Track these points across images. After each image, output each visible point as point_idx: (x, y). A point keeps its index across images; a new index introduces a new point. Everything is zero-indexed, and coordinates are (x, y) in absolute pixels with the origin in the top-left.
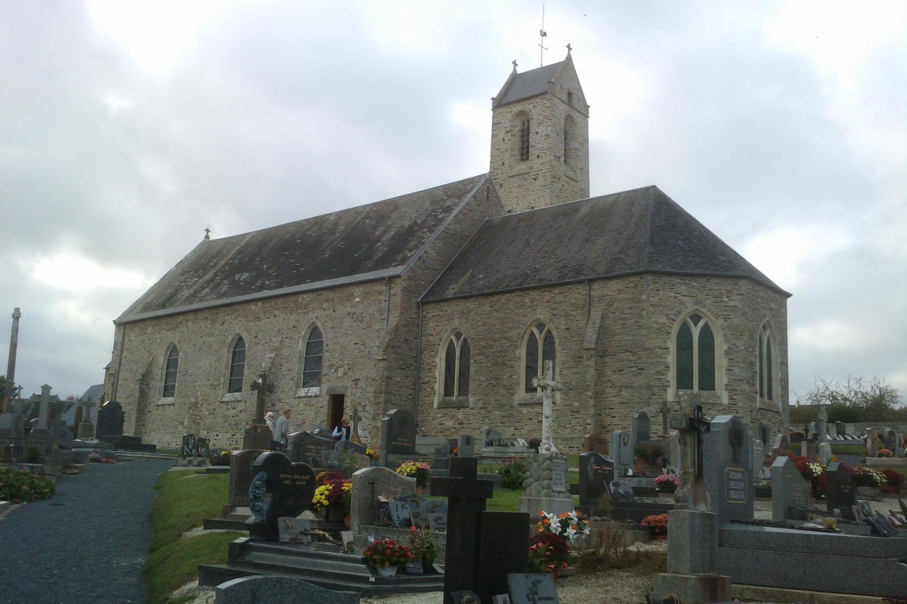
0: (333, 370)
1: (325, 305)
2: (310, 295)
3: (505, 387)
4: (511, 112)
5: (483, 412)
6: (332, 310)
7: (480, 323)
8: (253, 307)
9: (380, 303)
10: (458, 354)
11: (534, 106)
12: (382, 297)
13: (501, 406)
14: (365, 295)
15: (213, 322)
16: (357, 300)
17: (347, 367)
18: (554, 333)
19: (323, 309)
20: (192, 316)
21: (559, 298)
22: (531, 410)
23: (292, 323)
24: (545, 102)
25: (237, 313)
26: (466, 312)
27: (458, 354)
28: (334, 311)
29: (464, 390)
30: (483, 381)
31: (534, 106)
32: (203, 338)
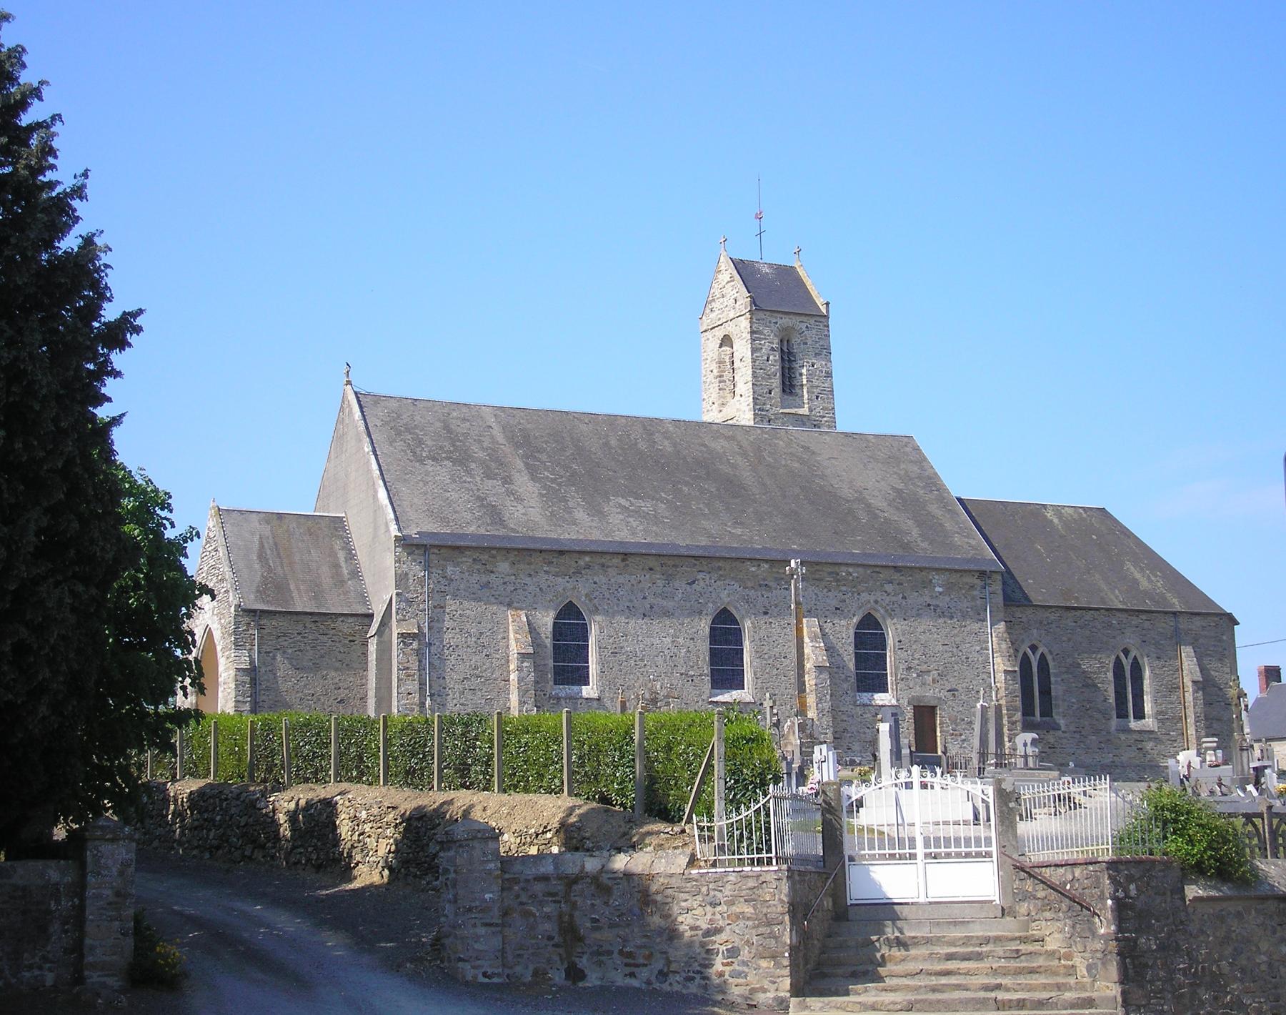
0: (915, 675)
1: (889, 588)
2: (860, 570)
3: (1099, 711)
4: (776, 323)
5: (1077, 736)
6: (901, 596)
7: (1064, 639)
8: (753, 569)
9: (974, 598)
10: (1035, 669)
11: (807, 327)
12: (976, 593)
13: (1096, 732)
14: (950, 587)
15: (669, 578)
16: (939, 589)
17: (935, 672)
18: (1049, 658)
19: (886, 592)
20: (616, 561)
21: (1147, 625)
22: (1129, 737)
23: (835, 603)
24: (821, 327)
25: (721, 573)
26: (1046, 623)
27: (1035, 669)
28: (904, 598)
29: (1047, 712)
30: (1073, 703)
31: (807, 327)
32: (651, 600)
